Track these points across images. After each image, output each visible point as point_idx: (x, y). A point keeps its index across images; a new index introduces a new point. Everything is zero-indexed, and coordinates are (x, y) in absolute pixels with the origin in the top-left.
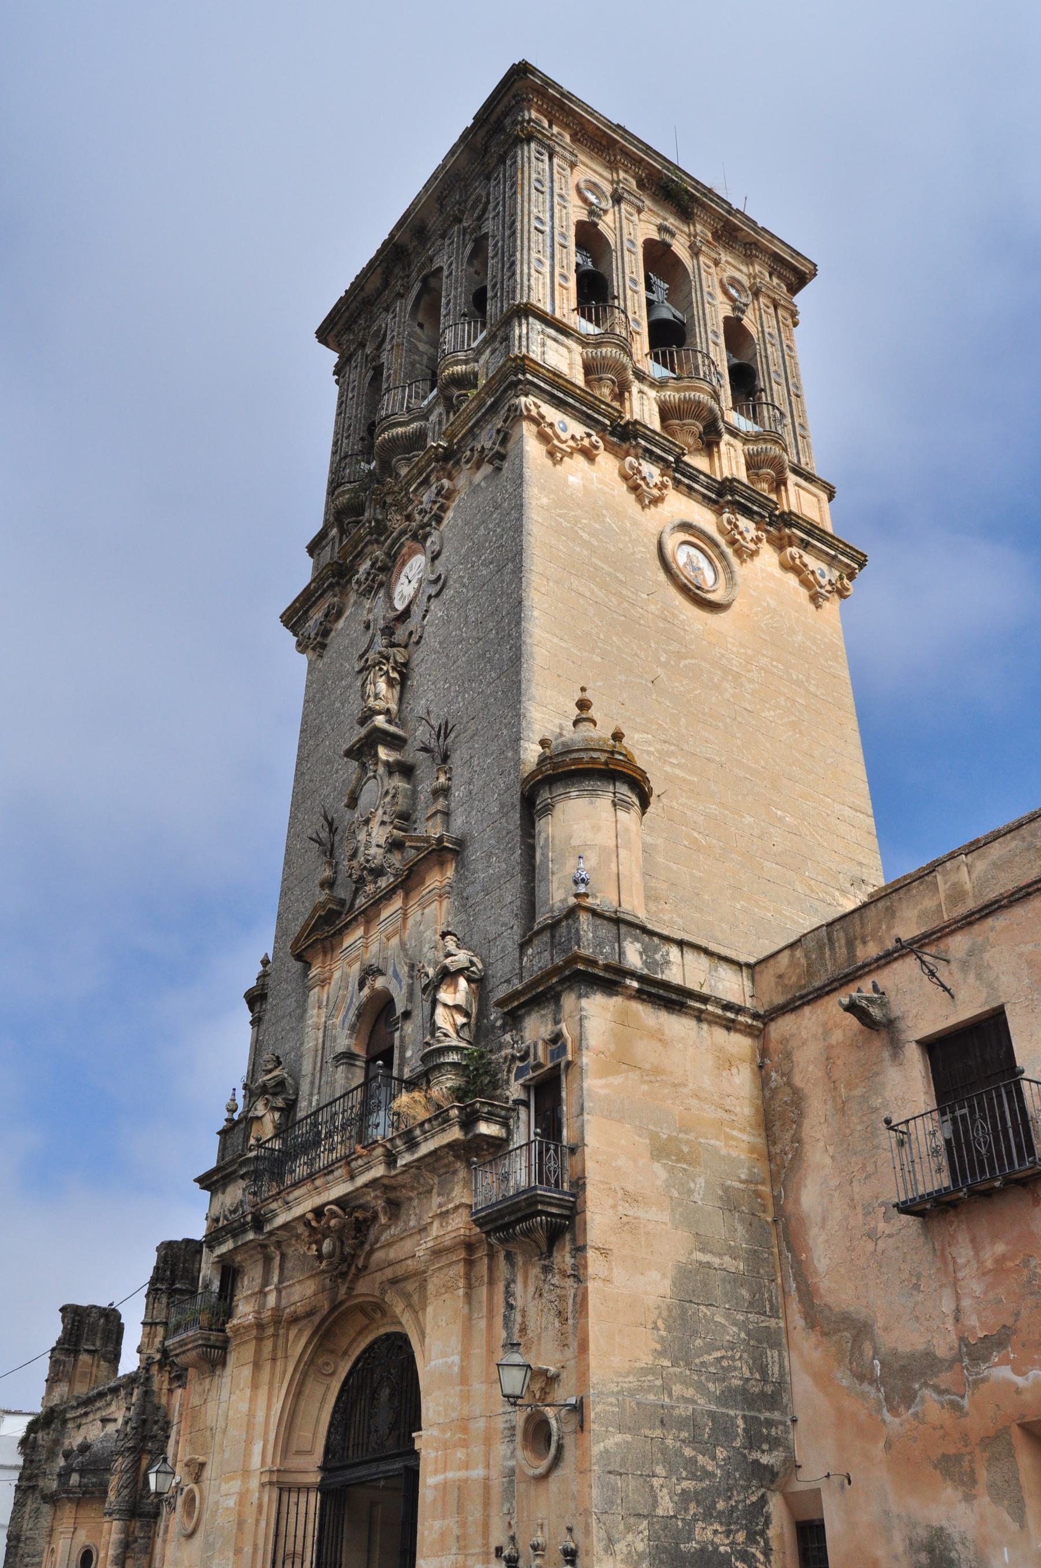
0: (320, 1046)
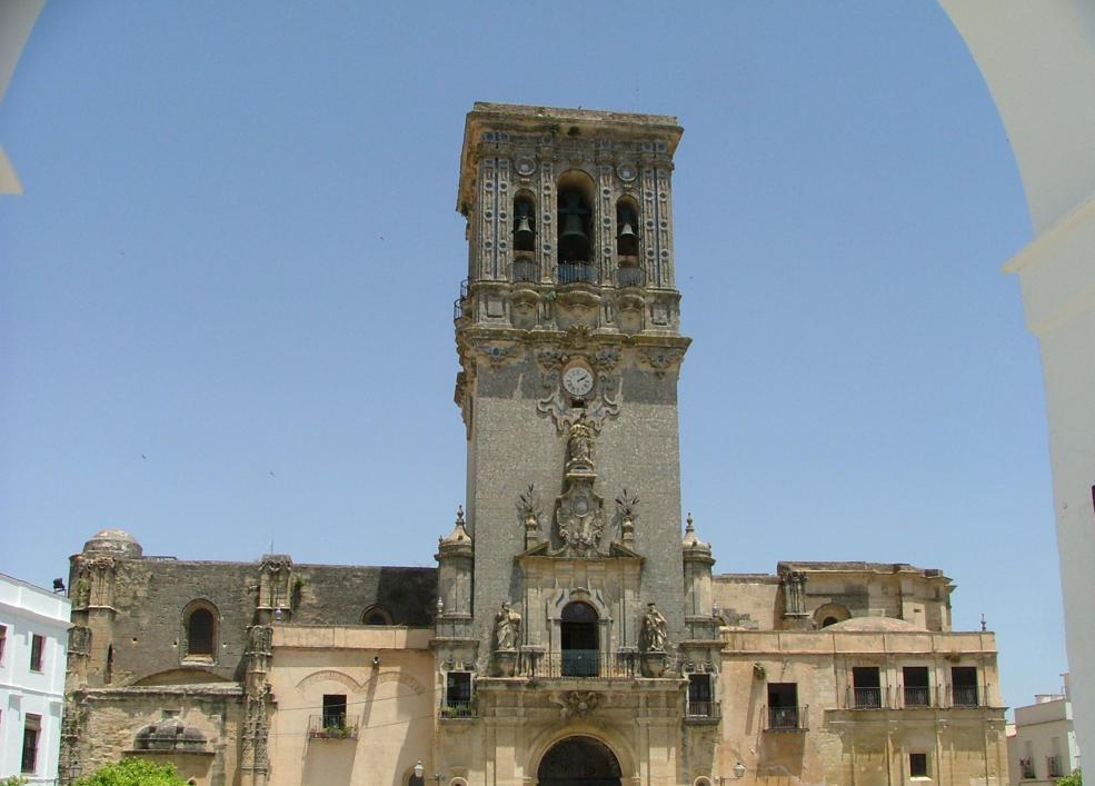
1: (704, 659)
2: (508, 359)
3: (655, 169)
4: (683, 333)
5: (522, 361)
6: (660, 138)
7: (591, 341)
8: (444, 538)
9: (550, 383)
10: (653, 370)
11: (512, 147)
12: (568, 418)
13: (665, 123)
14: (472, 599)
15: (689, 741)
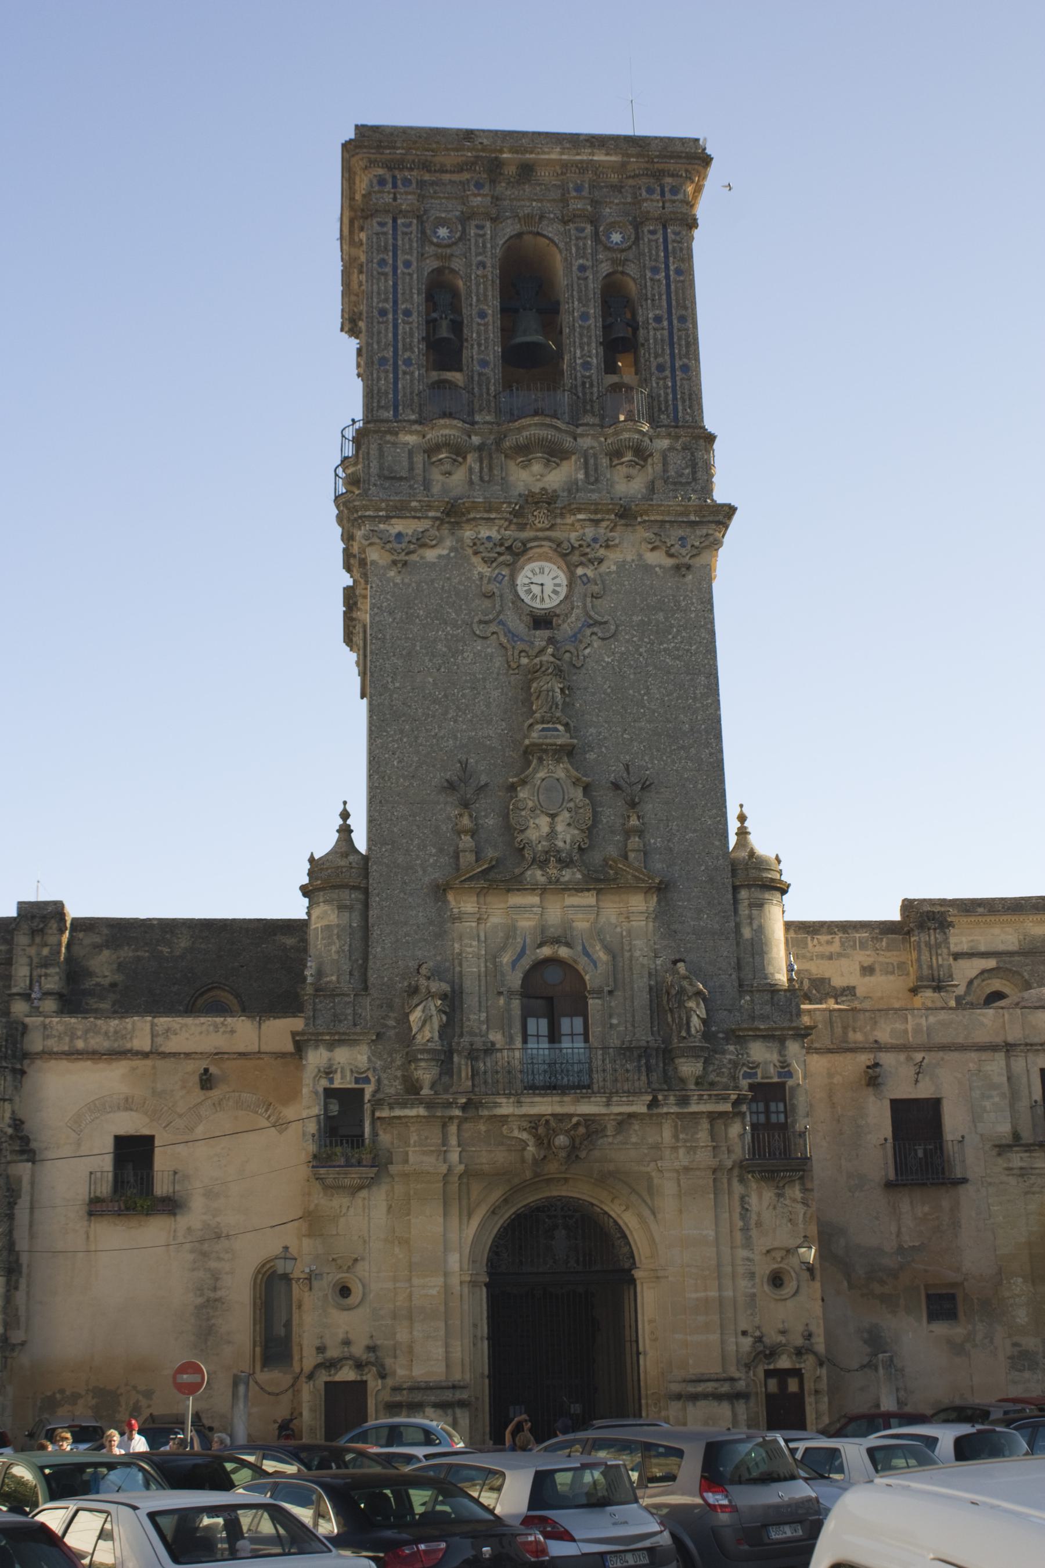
0: (483, 974)
1: (775, 1057)
2: (421, 551)
3: (665, 228)
4: (721, 495)
5: (445, 552)
6: (672, 176)
8: (316, 857)
9: (493, 587)
10: (669, 562)
11: (421, 198)
13: (679, 148)
14: (366, 959)
15: (753, 1200)
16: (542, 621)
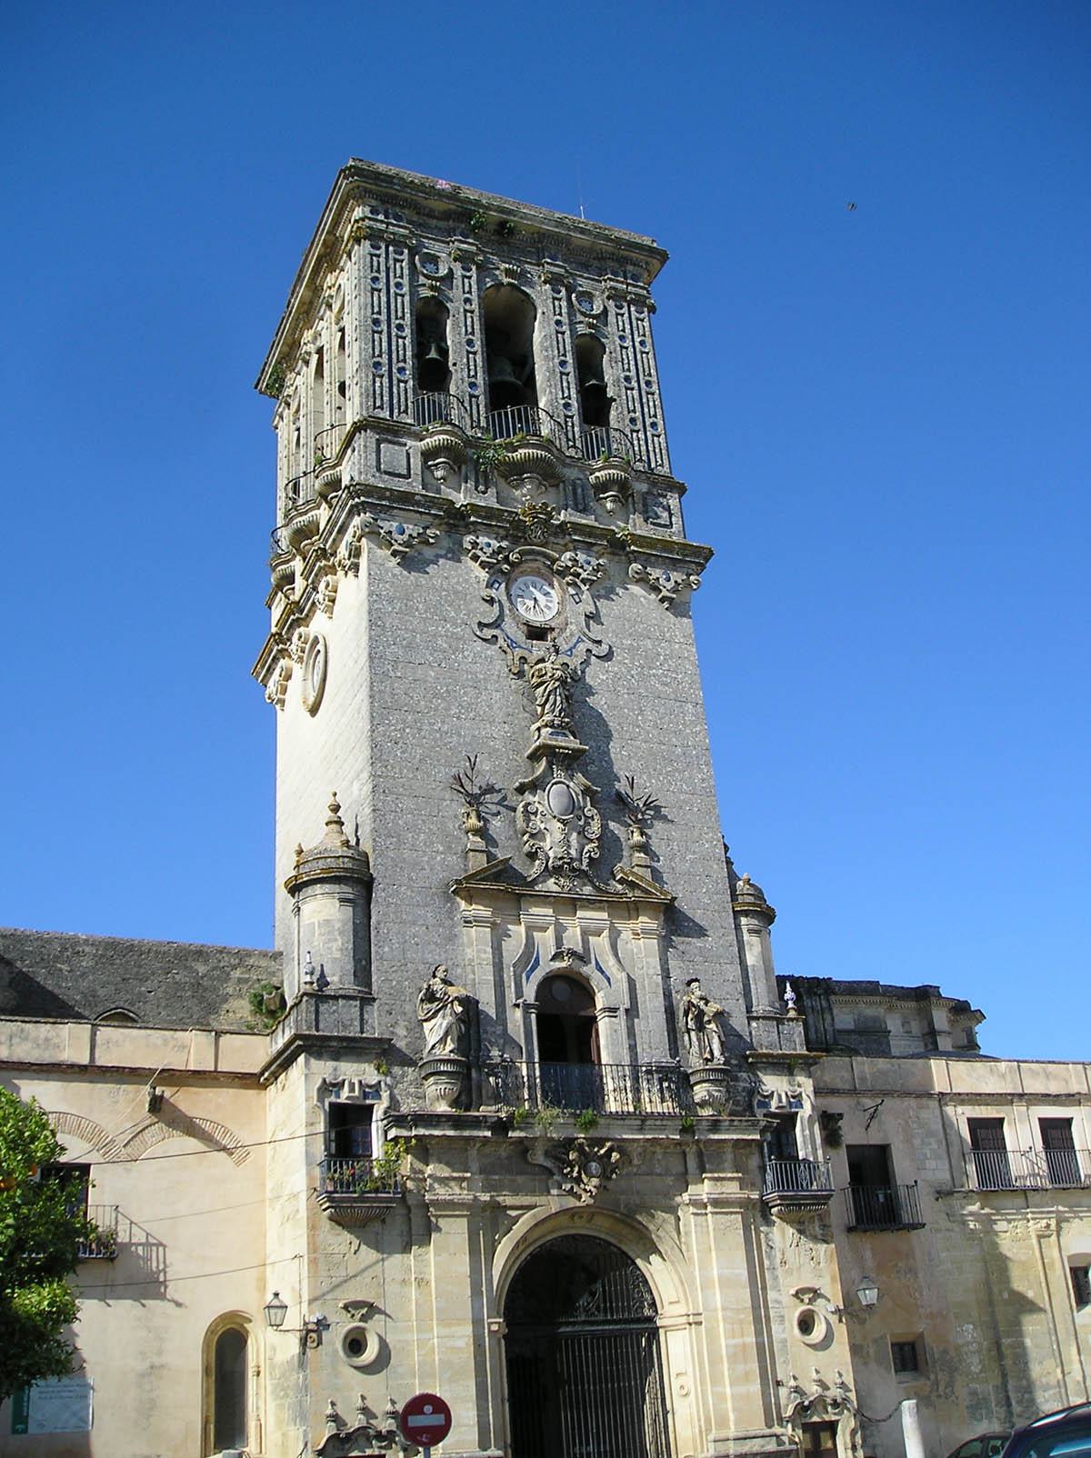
7: (555, 535)
12: (526, 653)
16: (537, 633)
